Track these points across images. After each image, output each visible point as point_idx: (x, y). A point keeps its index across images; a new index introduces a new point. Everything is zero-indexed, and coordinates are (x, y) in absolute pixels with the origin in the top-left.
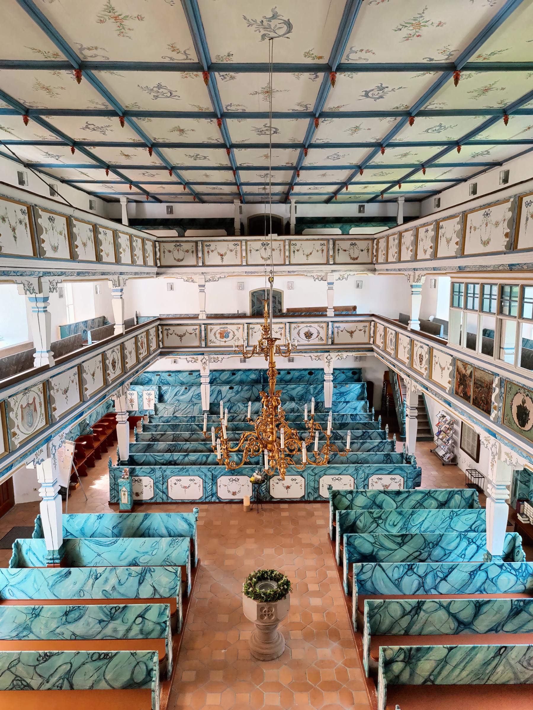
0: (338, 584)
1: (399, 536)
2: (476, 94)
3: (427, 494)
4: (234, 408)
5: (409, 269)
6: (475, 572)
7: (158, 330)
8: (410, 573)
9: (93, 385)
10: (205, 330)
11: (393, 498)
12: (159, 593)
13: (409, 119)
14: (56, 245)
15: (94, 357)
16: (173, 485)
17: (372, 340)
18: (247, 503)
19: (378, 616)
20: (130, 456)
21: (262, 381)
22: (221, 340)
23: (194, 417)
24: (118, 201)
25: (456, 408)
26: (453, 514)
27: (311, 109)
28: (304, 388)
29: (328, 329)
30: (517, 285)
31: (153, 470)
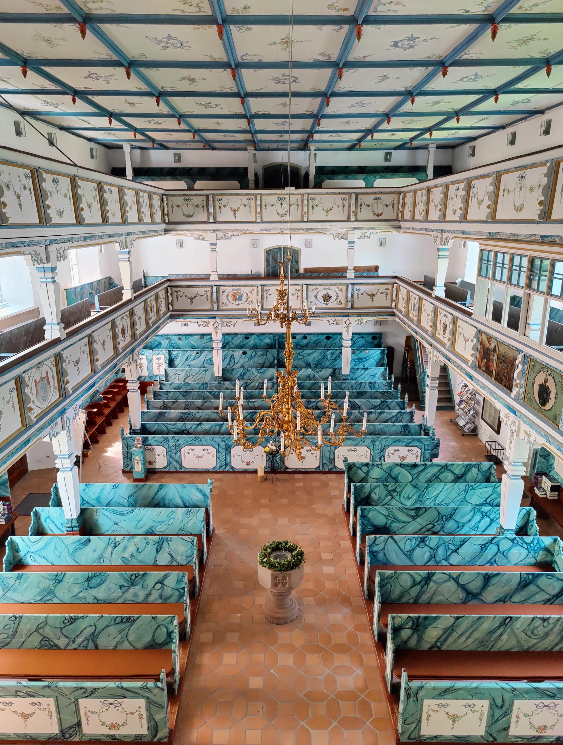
0: (352, 554)
1: (412, 510)
2: (515, 44)
3: (444, 467)
4: (248, 374)
5: (436, 230)
6: (487, 545)
7: (168, 292)
8: (422, 545)
9: (104, 354)
10: (217, 292)
11: (409, 470)
12: (176, 561)
13: (441, 69)
14: (61, 209)
15: (104, 325)
16: (186, 454)
17: (394, 303)
18: (261, 473)
19: (388, 586)
20: (142, 424)
21: (277, 346)
22: (234, 302)
23: (207, 383)
24: (121, 147)
25: (477, 382)
26: (469, 488)
27: (334, 58)
28: (321, 353)
29: (347, 292)
30: (548, 259)
31: (166, 439)
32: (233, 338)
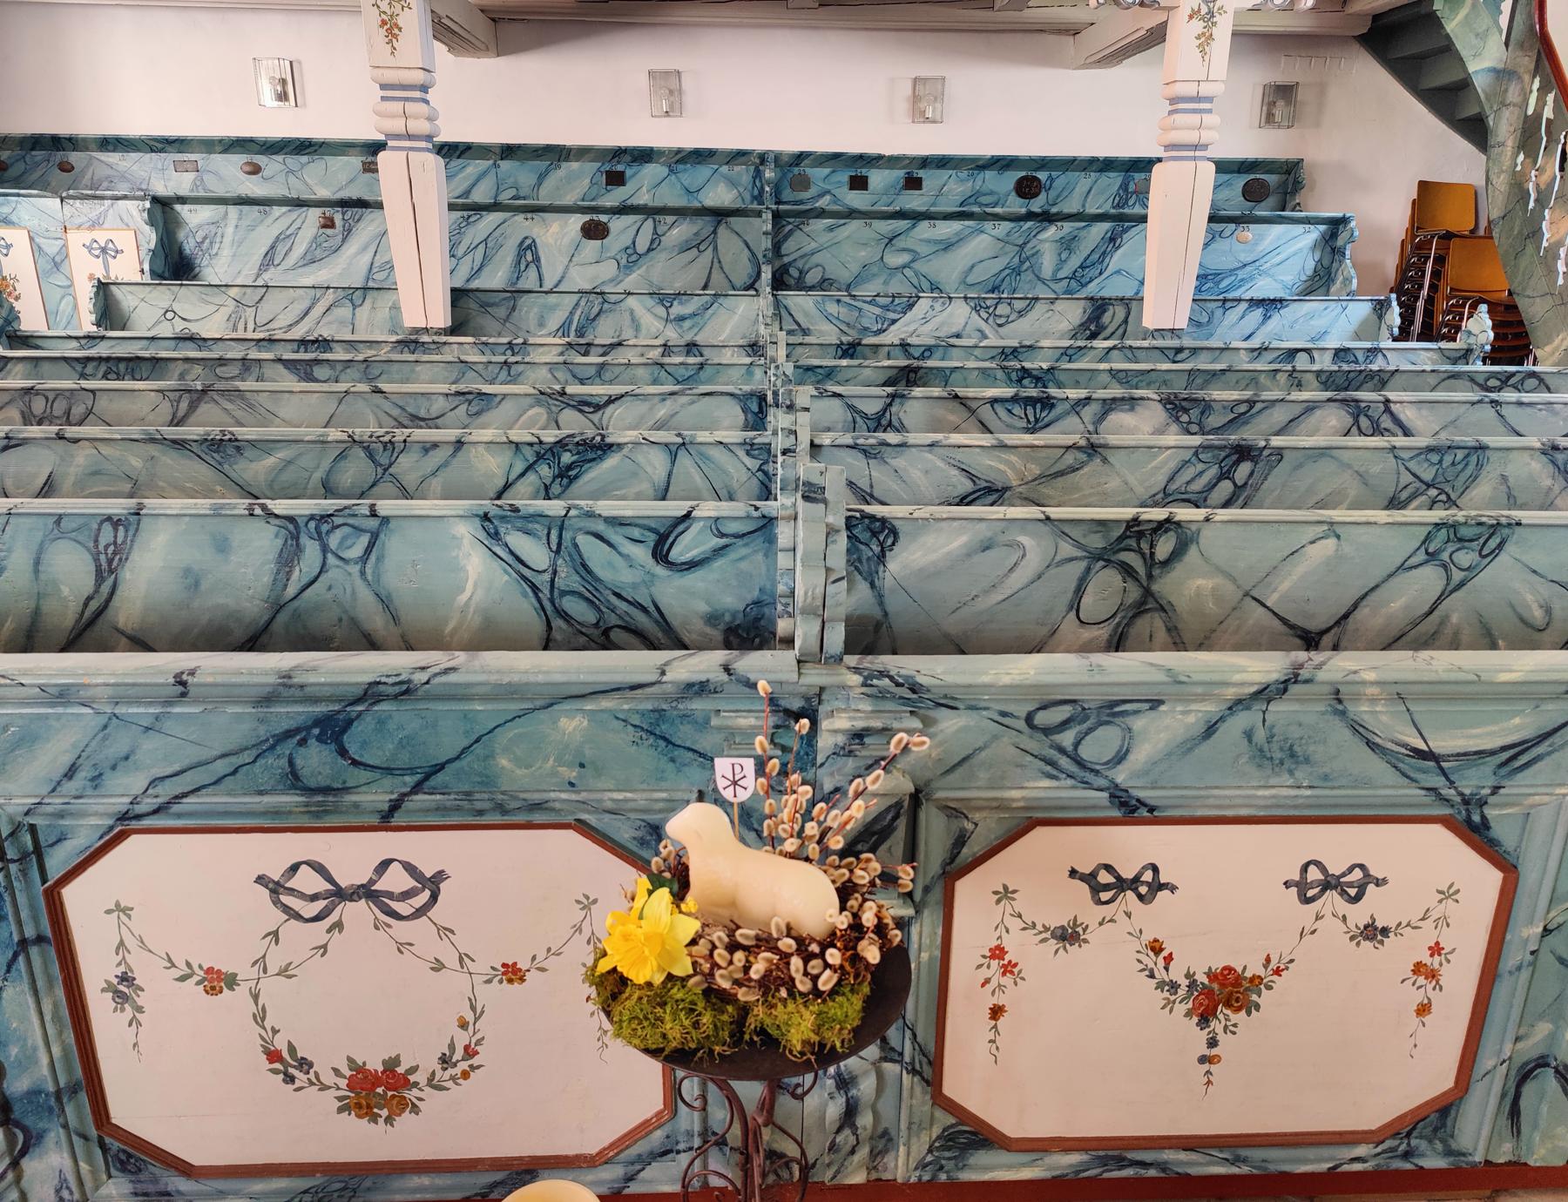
32: (542, 177)
